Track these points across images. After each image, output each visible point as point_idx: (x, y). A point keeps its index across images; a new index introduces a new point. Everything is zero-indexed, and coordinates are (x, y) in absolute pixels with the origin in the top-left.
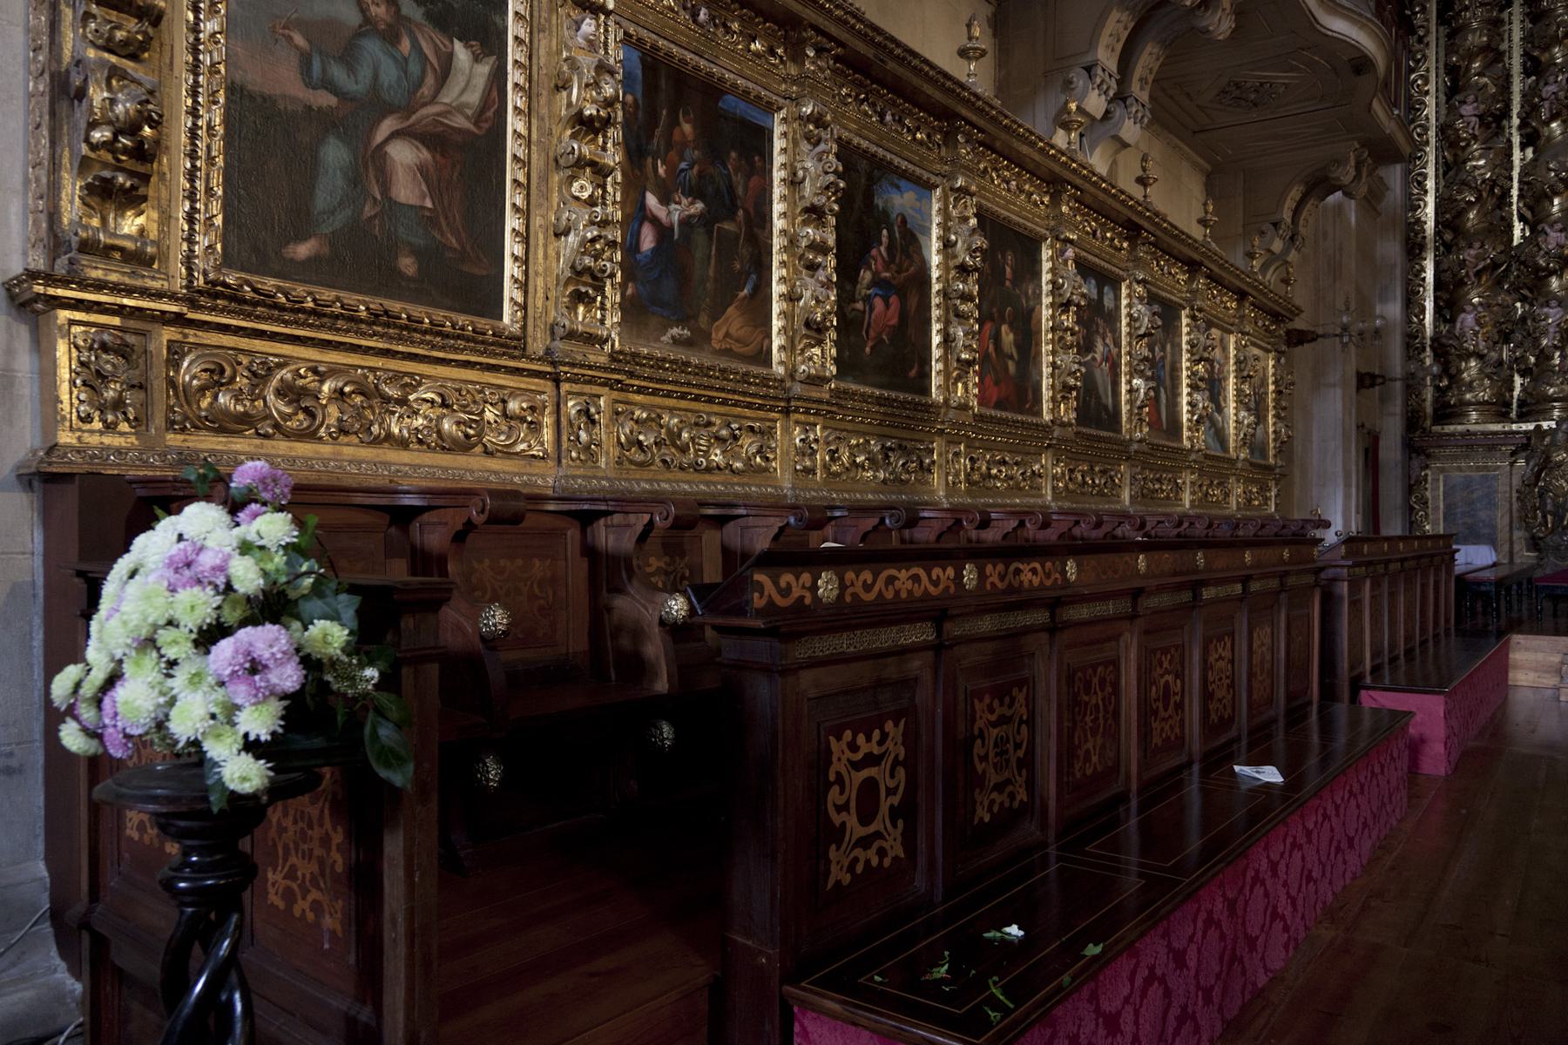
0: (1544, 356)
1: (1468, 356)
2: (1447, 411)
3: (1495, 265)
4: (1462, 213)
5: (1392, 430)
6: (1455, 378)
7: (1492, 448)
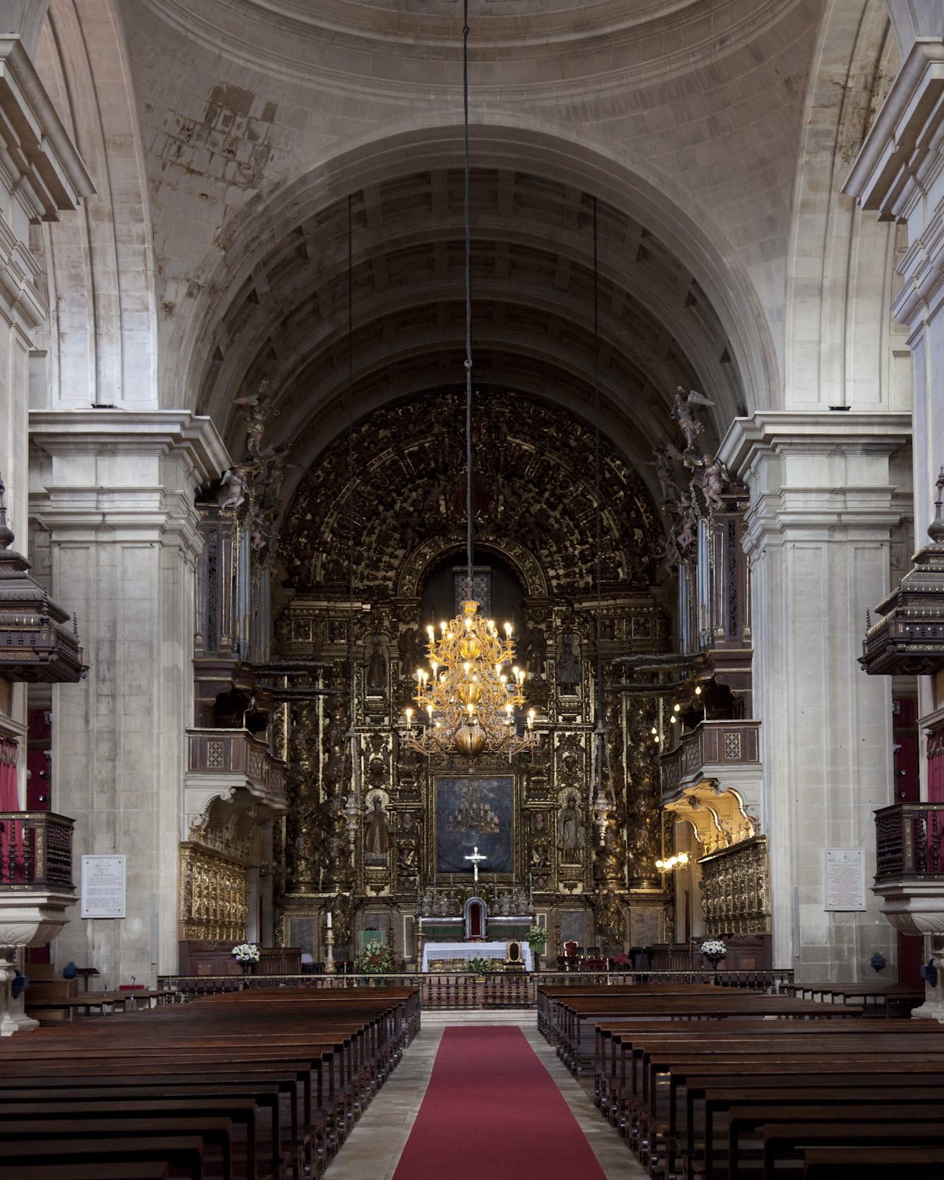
0: (332, 861)
1: (300, 858)
2: (292, 887)
3: (312, 814)
4: (298, 786)
5: (269, 893)
6: (295, 870)
7: (311, 906)
